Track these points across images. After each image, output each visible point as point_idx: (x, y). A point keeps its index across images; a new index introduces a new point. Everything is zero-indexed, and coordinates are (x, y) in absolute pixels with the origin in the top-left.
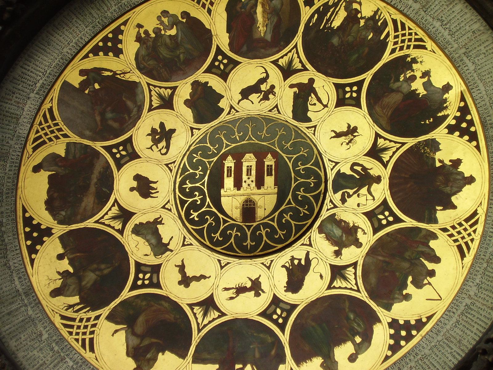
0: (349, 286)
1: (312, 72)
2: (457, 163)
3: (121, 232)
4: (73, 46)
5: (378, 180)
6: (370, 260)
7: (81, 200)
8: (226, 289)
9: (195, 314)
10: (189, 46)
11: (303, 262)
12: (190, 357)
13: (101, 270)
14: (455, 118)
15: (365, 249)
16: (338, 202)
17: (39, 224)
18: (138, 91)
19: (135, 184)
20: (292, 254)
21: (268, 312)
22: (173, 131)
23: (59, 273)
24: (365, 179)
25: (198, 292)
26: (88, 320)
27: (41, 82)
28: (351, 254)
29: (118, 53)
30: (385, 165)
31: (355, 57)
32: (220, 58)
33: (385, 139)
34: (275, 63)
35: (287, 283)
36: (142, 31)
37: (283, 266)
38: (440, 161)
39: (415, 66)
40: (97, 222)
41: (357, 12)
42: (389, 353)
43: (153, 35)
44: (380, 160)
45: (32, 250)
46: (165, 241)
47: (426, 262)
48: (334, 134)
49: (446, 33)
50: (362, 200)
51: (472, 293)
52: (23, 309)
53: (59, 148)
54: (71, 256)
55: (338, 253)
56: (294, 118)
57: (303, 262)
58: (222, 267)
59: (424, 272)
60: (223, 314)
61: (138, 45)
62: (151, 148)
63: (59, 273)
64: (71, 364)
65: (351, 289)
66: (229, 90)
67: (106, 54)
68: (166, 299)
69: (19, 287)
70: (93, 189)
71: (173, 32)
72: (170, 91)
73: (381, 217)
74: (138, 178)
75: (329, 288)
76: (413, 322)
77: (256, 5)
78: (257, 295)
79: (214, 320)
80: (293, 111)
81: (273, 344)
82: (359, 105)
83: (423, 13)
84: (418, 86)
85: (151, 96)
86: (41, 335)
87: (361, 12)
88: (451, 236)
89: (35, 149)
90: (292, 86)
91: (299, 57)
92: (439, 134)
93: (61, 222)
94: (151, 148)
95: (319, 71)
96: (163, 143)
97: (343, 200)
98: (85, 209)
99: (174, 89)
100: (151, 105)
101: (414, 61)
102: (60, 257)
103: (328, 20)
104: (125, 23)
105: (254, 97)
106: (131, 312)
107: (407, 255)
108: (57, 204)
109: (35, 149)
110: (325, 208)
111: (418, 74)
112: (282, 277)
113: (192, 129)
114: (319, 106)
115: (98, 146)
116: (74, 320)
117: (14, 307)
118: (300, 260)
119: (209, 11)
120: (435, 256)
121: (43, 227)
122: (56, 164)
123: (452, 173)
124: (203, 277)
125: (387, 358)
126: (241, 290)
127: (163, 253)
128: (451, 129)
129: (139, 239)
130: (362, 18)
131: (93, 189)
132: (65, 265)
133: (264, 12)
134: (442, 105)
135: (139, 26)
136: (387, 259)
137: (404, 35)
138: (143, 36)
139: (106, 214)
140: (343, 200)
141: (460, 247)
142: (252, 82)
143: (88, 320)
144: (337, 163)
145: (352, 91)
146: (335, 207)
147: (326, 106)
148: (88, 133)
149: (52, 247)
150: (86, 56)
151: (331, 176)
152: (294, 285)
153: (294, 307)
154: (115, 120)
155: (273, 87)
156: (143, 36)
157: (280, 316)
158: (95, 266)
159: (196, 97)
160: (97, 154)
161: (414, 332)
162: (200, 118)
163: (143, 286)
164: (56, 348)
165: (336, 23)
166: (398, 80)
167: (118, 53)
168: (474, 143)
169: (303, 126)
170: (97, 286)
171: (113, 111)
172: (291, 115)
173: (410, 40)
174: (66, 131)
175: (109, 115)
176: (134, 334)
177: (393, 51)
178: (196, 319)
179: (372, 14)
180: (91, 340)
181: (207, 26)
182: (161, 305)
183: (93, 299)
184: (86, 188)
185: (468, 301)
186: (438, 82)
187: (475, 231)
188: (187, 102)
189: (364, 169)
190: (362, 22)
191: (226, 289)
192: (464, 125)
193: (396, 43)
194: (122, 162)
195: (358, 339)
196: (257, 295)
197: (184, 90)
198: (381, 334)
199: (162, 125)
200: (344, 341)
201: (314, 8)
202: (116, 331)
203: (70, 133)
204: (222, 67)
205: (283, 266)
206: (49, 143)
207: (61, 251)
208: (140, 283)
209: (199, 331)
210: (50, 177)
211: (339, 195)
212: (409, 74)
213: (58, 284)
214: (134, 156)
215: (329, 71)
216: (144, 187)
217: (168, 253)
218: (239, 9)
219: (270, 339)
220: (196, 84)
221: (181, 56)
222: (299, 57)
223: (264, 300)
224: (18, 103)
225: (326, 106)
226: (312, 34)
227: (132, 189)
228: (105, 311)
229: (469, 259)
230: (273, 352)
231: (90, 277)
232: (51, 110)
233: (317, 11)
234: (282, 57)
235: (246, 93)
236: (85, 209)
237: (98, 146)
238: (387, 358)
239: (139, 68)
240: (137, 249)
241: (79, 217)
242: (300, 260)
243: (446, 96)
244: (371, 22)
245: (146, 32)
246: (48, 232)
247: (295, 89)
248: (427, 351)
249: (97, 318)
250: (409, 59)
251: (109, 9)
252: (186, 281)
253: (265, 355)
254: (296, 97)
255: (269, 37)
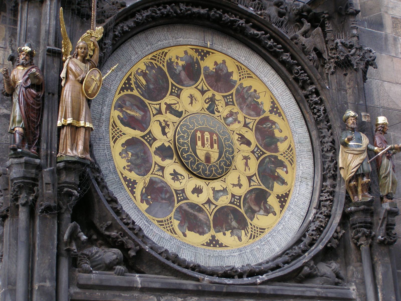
0: (253, 123)
1: (162, 102)
2: (216, 63)
3: (216, 206)
4: (130, 202)
5: (214, 95)
6: (244, 111)
7: (200, 220)
8: (245, 170)
9: (254, 185)
10: (138, 150)
11: (240, 137)
12: (270, 192)
13: (231, 218)
14: (198, 55)
15: (239, 111)
16: (219, 114)
17: (210, 240)
18: (154, 179)
19: (196, 194)
20: (236, 139)
21: (257, 156)
22: (174, 170)
23: (231, 236)
24: (212, 100)
25: (244, 181)
26: (252, 228)
27: (145, 222)
28: (240, 117)
29: (135, 182)
30: (209, 90)
31: (161, 82)
32: (146, 138)
33: (198, 85)
34: (154, 115)
35: (247, 145)
36: (126, 168)
37: (240, 145)
38: (213, 69)
39: (172, 60)
40: (211, 215)
41: (142, 71)
42: (281, 117)
43: (130, 163)
44: (206, 91)
45: (221, 245)
46: (222, 189)
47: (251, 91)
48: (191, 105)
49: (165, 41)
50: (220, 105)
51: (267, 80)
52: (247, 254)
53: (176, 223)
54: (224, 230)
55: (239, 122)
56: (180, 117)
57: (240, 137)
58: (236, 169)
59: (254, 93)
60: (255, 174)
61: (133, 172)
62: (181, 183)
63: (231, 236)
64: (270, 238)
65: (254, 122)
66: (162, 140)
67: (135, 188)
68: (246, 195)
69: (237, 254)
70: (196, 213)
71: (130, 154)
72: (156, 166)
73: (229, 100)
74: (193, 192)
75: (252, 130)
76: (272, 105)
77: (126, 112)
78: (250, 158)
79: (257, 178)
80: (177, 116)
81: (269, 159)
82: (181, 90)
83: (153, 46)
84: (181, 63)
85: (157, 175)
86: (258, 248)
87: (143, 70)
88: (243, 78)
89: (176, 234)
90: (166, 113)
91: (154, 104)
92: (203, 64)
93: (209, 230)
94: (181, 183)
95: (162, 99)
96: (179, 176)
97: (219, 112)
98: (205, 219)
99: (156, 163)
100: (161, 176)
101: (170, 59)
102: (224, 234)
103: (142, 85)
104: (122, 174)
105: (167, 130)
106: (250, 210)
107: (246, 97)
108: (201, 230)
109: (176, 234)
110: (220, 120)
111: (176, 60)
112: (244, 147)
113: (175, 162)
114: (177, 105)
115: (177, 205)
116: (251, 234)
117: (245, 257)
118: (239, 137)
119: (124, 134)
120: (249, 87)
121: (211, 239)
122: (183, 226)
123: (219, 67)
124: (239, 178)
125: (283, 119)
126: (246, 164)
127: (227, 191)
128: (202, 59)
129: (220, 199)
130: (145, 71)
131: (196, 213)
132: (228, 233)
133: (130, 110)
134: (192, 58)
135: (124, 168)
136: (246, 105)
137: (158, 58)
138: (129, 168)
139: (207, 210)
140: (219, 112)
141: (248, 77)
142: (160, 129)
143: (252, 228)
144: (203, 108)
145: (175, 90)
146: (220, 116)
147: (178, 103)
148: (170, 208)
149: (219, 236)
150: (135, 197)
151: (207, 112)
152: (248, 143)
153: (257, 146)
154: (166, 194)
155: (164, 121)
156: (129, 168)
157: (259, 153)
158: (229, 221)
159: (161, 155)
160: (180, 207)
161: (276, 106)
162: (171, 157)
163: (240, 203)
164: (264, 243)
165: (144, 82)
166: (176, 69)
167: (135, 182)
168: (211, 53)
169: (184, 115)
170: (238, 222)
171: (162, 193)
172: (178, 118)
173: (161, 57)
174: (168, 217)
175: (163, 196)
176: (259, 211)
177: (163, 65)
178: (255, 185)
179: (145, 66)
180: (260, 229)
181: (131, 138)
182: (248, 197)
183: (243, 224)
184: (195, 217)
185: (269, 82)
186: (182, 55)
187: (244, 69)
188: (163, 160)
189: (208, 99)
190: (147, 72)
191: (245, 170)
192: (202, 54)
193: (161, 63)
194: (185, 197)
195: (274, 126)
196: (250, 158)
197: (157, 159)
198: (273, 117)
199: (171, 174)
200: (273, 132)
201: (135, 88)
202: (257, 218)
203: (170, 216)
204: (150, 139)
205: (240, 145)
206: (173, 226)
207: (222, 233)
208: (238, 204)
209: (260, 185)
210: (189, 230)
211: (216, 113)
212: (175, 64)
213: (236, 237)
214: (183, 191)
215: (164, 95)
216: (197, 191)
217: (227, 189)
218: (126, 121)
219: (267, 159)
220: (155, 153)
221: (142, 154)
222: (154, 104)
223: (251, 156)
224: (153, 235)
225: (178, 103)
226: (146, 94)
227: (198, 196)
228: (249, 221)
229: (253, 76)
230: (273, 159)
231: (234, 224)
232: (158, 221)
233: (136, 88)
234: (152, 111)
235: (164, 133)
236: (205, 219)
237: (177, 205)
238: (283, 119)
239: (144, 175)
240: (224, 201)
241: (208, 222)
242: (239, 137)
243: (189, 54)
244: (149, 68)
245: (128, 166)
246: (213, 237)
247: (168, 112)
248: (284, 104)
249: (251, 224)
250: (169, 61)
251: (114, 179)
252: (240, 186)
253: (273, 163)
254: (171, 113)
255: (142, 113)
